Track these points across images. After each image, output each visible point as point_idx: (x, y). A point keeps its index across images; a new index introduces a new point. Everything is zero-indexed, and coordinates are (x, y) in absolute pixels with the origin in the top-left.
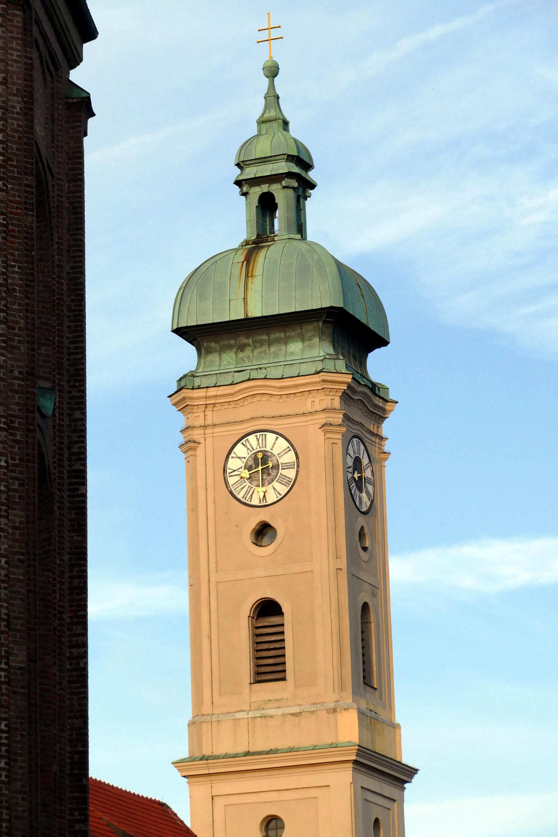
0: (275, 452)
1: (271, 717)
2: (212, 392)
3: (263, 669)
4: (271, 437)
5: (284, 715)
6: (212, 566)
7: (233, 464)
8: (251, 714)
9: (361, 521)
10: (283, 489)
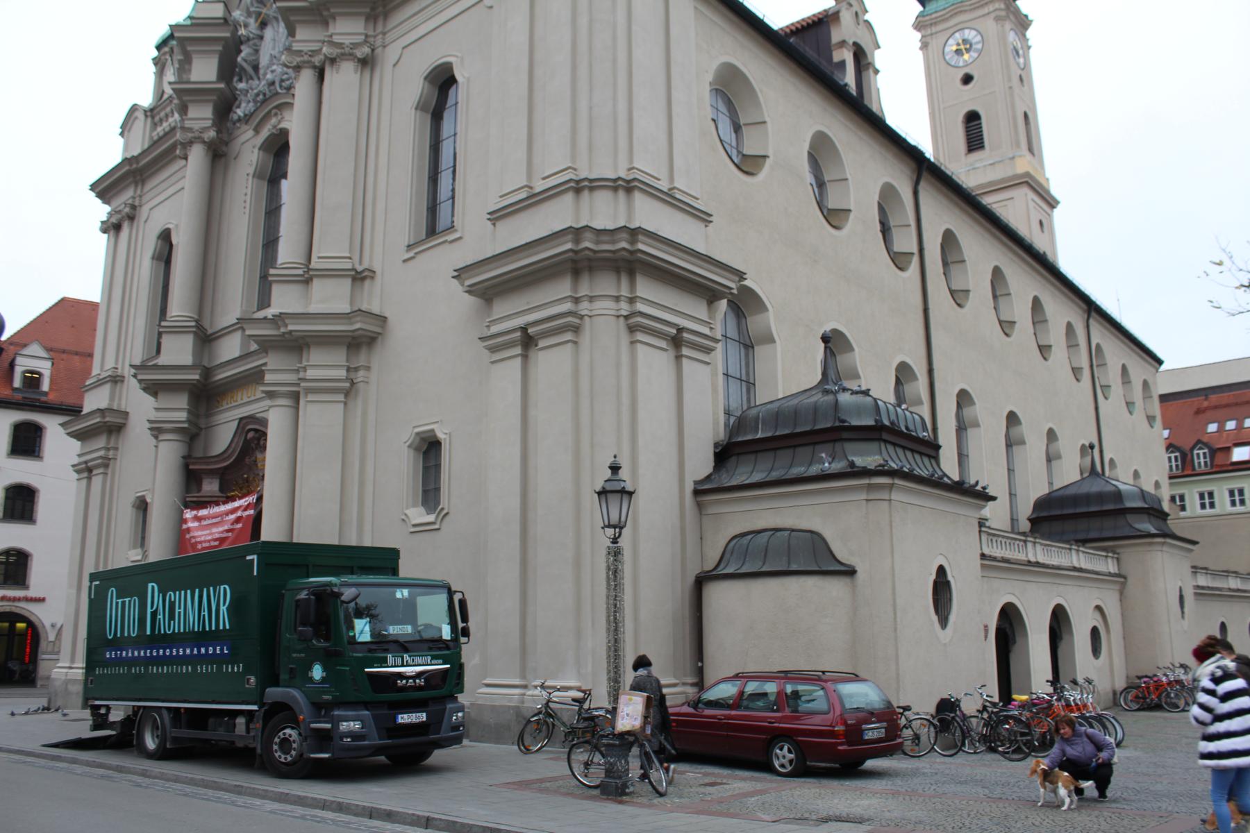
0: (970, 37)
1: (978, 168)
2: (934, 16)
3: (972, 148)
4: (967, 31)
5: (985, 166)
6: (940, 99)
7: (947, 49)
8: (967, 169)
9: (1019, 72)
10: (975, 55)
